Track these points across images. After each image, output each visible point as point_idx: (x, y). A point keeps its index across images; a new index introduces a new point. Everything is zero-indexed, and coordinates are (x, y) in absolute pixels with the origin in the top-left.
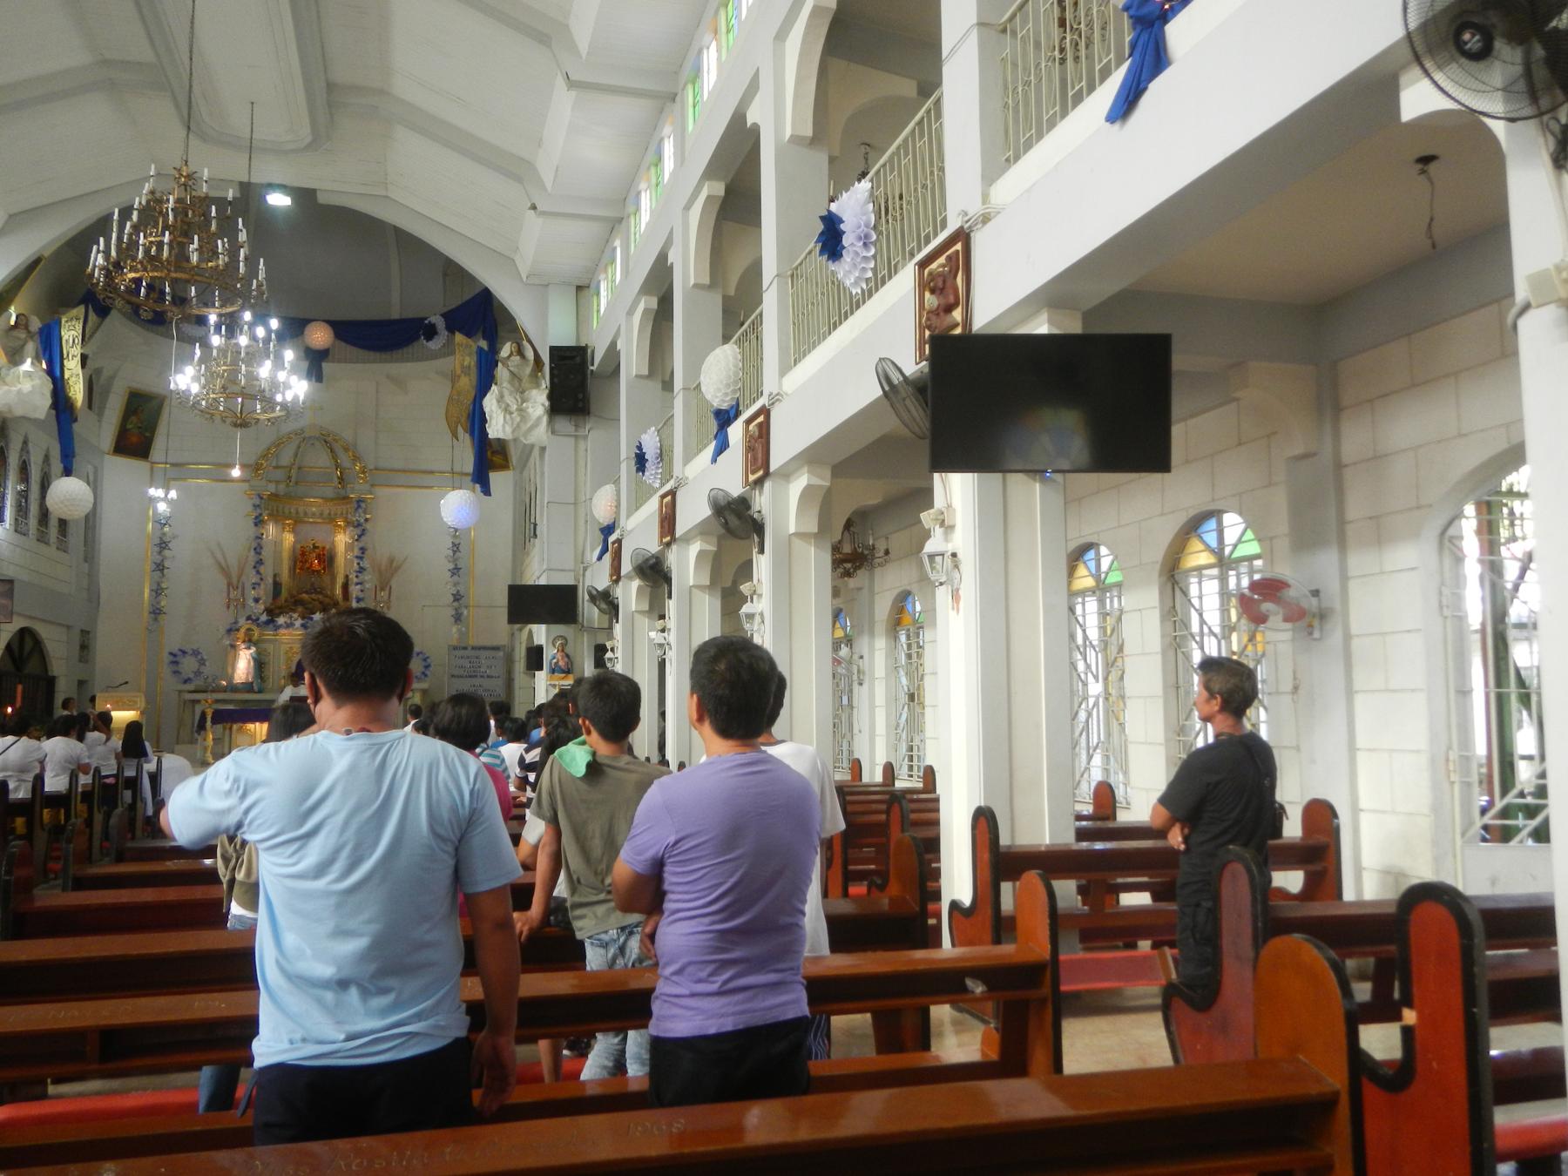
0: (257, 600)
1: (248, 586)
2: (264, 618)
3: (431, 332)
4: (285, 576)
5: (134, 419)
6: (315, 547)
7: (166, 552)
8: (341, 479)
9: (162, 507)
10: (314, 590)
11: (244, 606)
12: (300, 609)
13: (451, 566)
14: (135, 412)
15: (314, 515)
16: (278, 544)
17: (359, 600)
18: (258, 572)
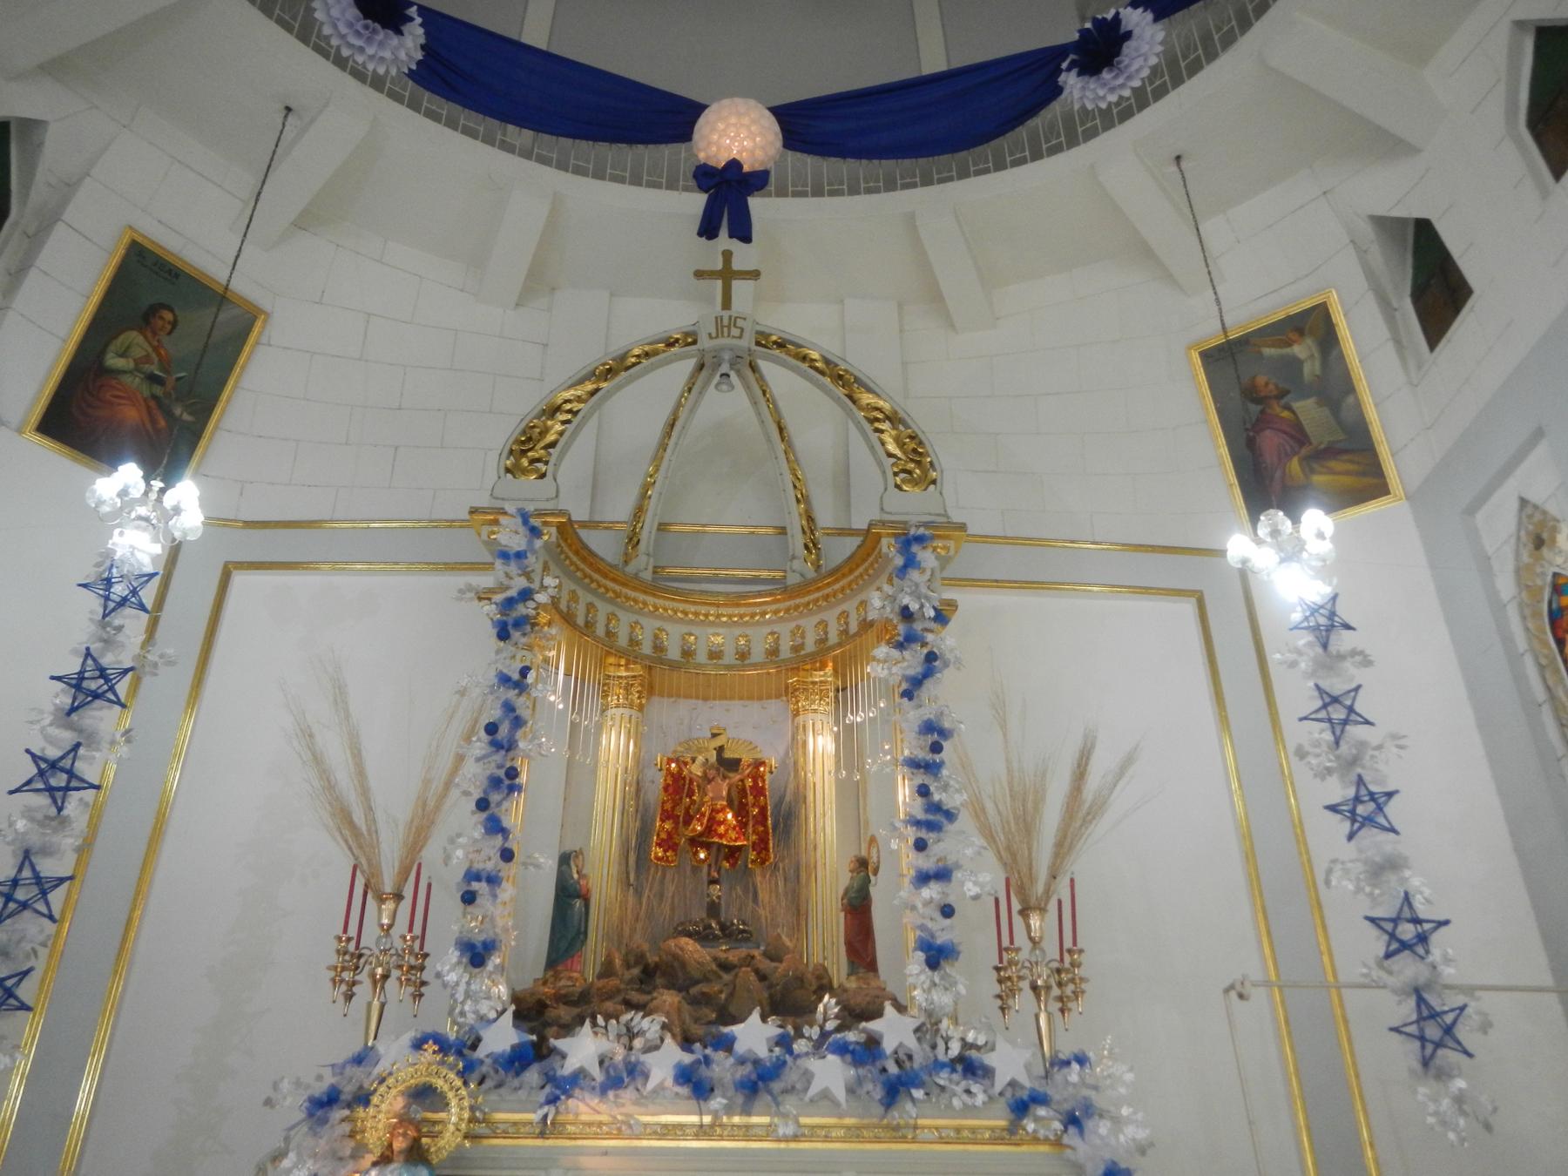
0: (476, 955)
1: (446, 905)
2: (503, 1037)
3: (1100, 48)
4: (602, 875)
5: (134, 337)
6: (728, 765)
7: (103, 718)
8: (812, 546)
9: (137, 548)
10: (716, 928)
11: (415, 970)
12: (669, 998)
13: (1339, 791)
14: (147, 319)
15: (715, 655)
16: (580, 740)
17: (937, 956)
18: (495, 827)
